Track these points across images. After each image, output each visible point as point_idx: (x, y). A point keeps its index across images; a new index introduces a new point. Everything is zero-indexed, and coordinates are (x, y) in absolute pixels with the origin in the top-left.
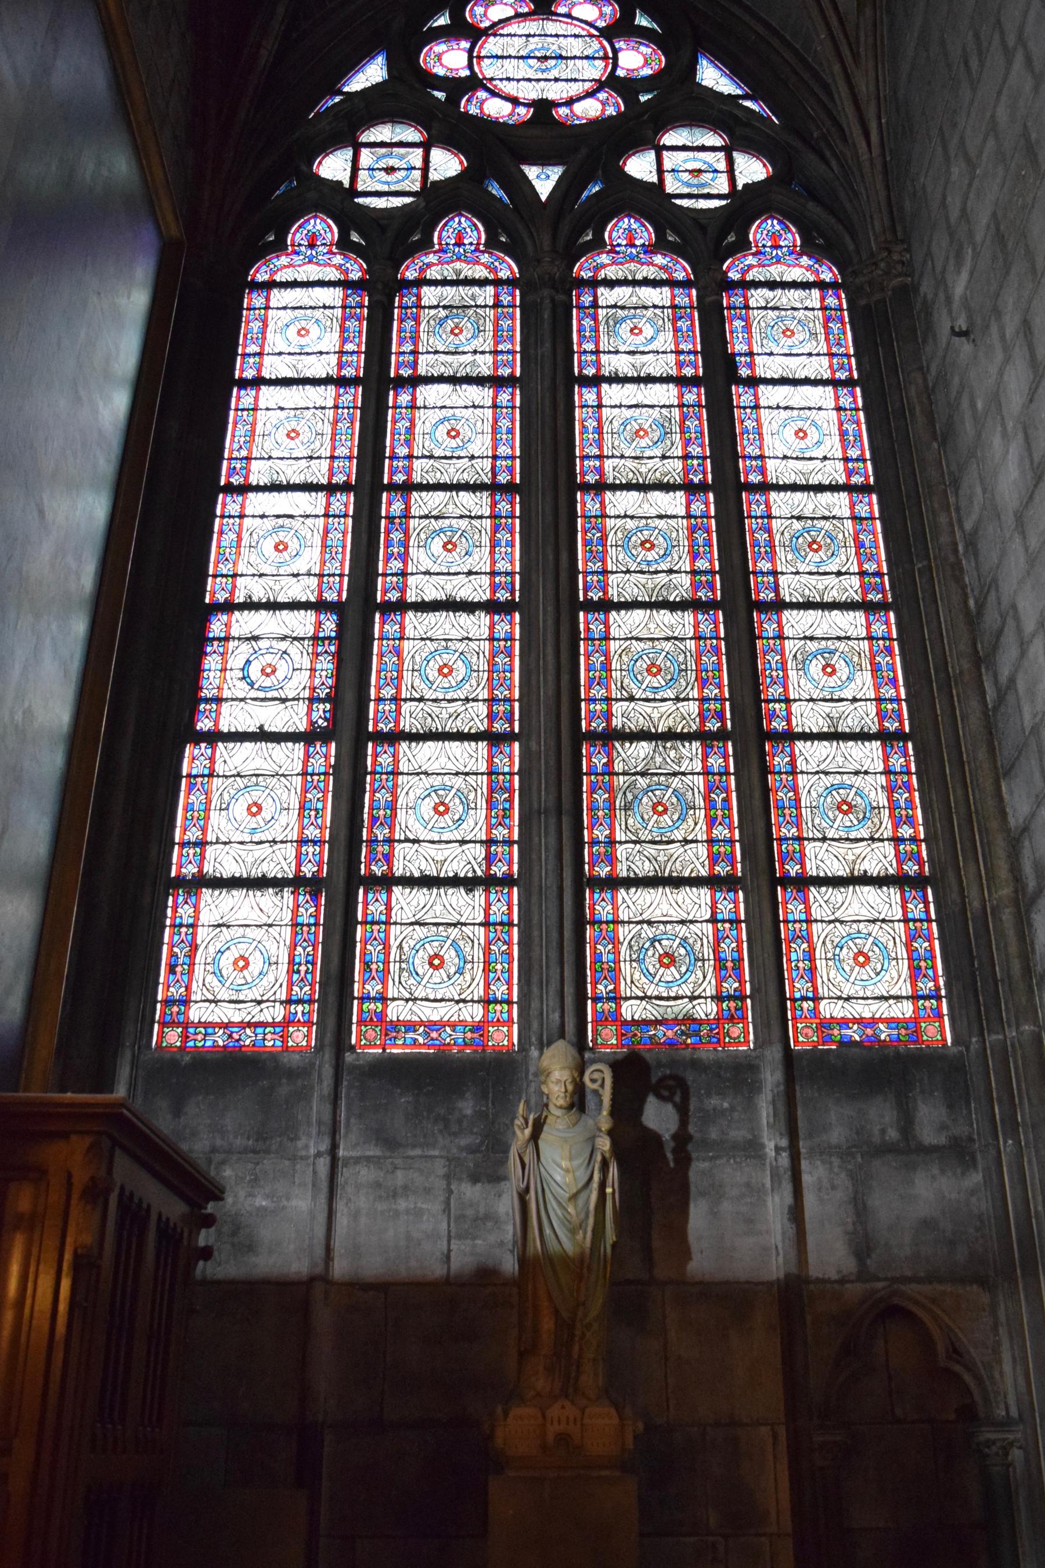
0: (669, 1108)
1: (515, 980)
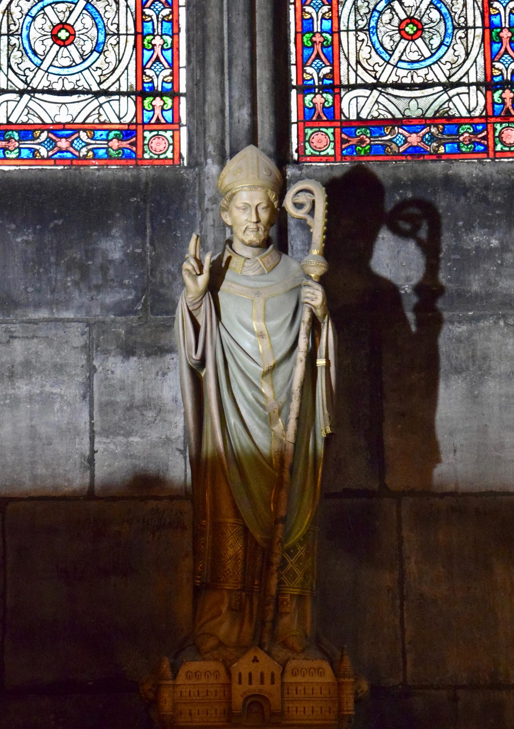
0: (412, 246)
1: (183, 62)
